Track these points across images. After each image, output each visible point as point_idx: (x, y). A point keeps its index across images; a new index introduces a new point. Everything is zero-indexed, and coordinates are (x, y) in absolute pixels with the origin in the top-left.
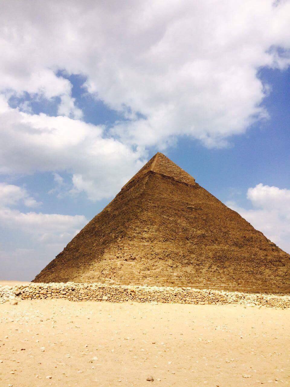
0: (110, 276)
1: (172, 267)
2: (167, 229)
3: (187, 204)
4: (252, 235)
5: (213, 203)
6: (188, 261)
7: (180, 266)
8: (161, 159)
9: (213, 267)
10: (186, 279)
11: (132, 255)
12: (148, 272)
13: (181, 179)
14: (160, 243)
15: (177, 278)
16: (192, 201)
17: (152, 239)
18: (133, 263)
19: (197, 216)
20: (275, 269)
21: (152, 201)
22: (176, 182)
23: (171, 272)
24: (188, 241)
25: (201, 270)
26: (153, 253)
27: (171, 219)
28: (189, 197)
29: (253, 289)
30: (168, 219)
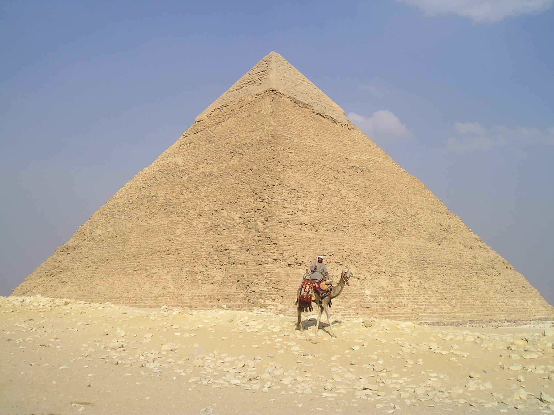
5: (381, 160)
6: (376, 267)
7: (369, 277)
11: (296, 257)
15: (372, 299)
19: (368, 184)
22: (317, 114)
23: (361, 289)
29: (474, 315)
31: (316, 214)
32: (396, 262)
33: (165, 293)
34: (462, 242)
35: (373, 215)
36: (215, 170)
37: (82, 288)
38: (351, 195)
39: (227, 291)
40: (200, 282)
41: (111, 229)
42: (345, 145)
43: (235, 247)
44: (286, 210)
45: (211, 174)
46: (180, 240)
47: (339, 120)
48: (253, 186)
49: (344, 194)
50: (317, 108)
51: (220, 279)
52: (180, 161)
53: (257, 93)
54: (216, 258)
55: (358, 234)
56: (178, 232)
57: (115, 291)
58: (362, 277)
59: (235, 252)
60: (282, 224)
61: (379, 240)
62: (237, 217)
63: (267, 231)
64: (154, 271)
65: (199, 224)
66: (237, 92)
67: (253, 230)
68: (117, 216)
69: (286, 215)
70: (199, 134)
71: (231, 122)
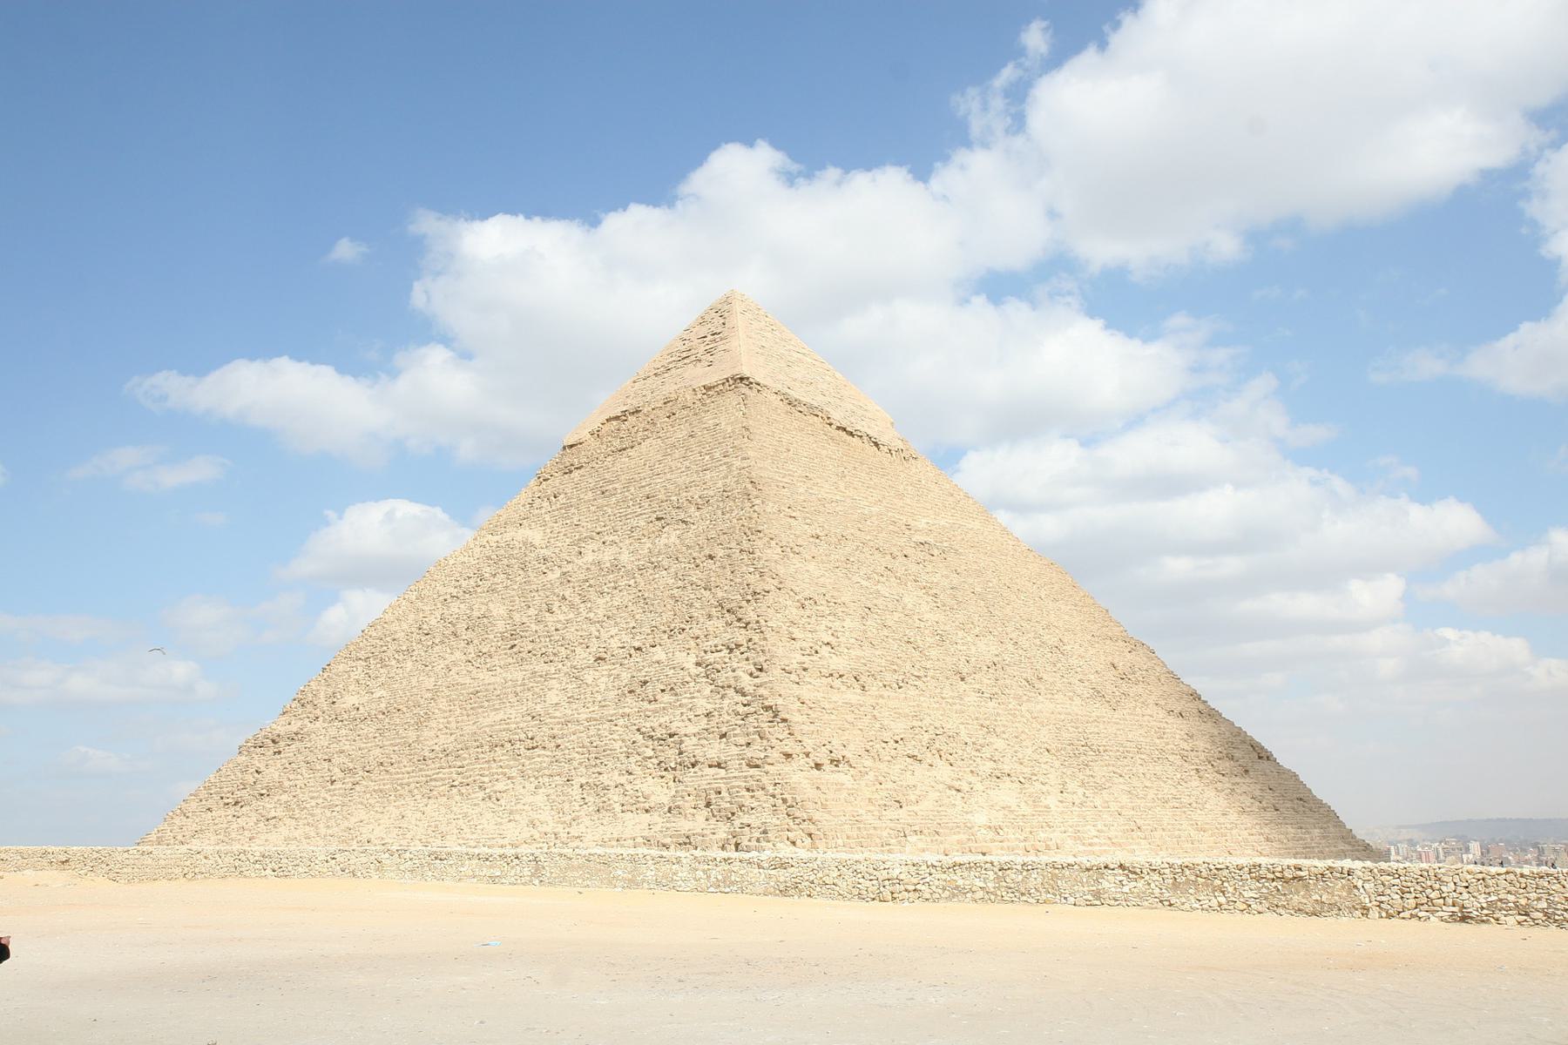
6: (991, 764)
15: (991, 834)
19: (956, 580)
31: (859, 653)
32: (1029, 751)
33: (537, 836)
35: (973, 649)
36: (625, 558)
37: (323, 831)
38: (925, 608)
39: (684, 826)
40: (618, 808)
41: (383, 693)
42: (901, 496)
43: (692, 729)
44: (798, 645)
45: (616, 567)
46: (558, 714)
47: (882, 440)
48: (720, 594)
49: (910, 606)
51: (666, 800)
52: (536, 536)
53: (707, 383)
54: (650, 753)
55: (947, 693)
56: (552, 697)
57: (409, 836)
58: (965, 787)
59: (695, 740)
60: (793, 677)
63: (762, 691)
64: (500, 786)
65: (600, 679)
66: (659, 380)
67: (731, 692)
68: (394, 662)
70: (576, 474)
71: (650, 448)
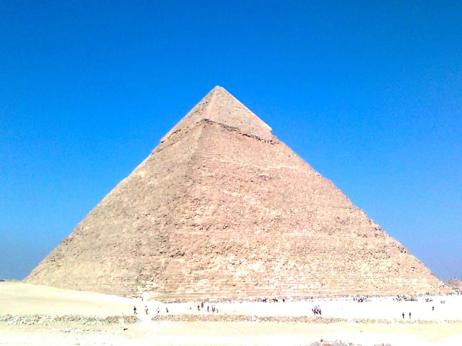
0: (152, 278)
1: (233, 264)
2: (228, 210)
3: (259, 170)
4: (349, 214)
5: (297, 167)
6: (256, 255)
8: (221, 98)
9: (290, 262)
10: (253, 280)
11: (180, 250)
12: (201, 272)
13: (251, 131)
14: (219, 231)
15: (240, 279)
16: (265, 165)
17: (208, 226)
18: (181, 260)
19: (273, 188)
20: (376, 262)
21: (207, 169)
22: (243, 135)
24: (258, 228)
25: (273, 268)
26: (208, 246)
27: (234, 194)
28: (262, 158)
29: (342, 291)
30: (231, 196)
34: (357, 232)
44: (184, 215)
50: (243, 131)
60: (177, 227)
61: (266, 234)
62: (153, 219)
69: (183, 220)
